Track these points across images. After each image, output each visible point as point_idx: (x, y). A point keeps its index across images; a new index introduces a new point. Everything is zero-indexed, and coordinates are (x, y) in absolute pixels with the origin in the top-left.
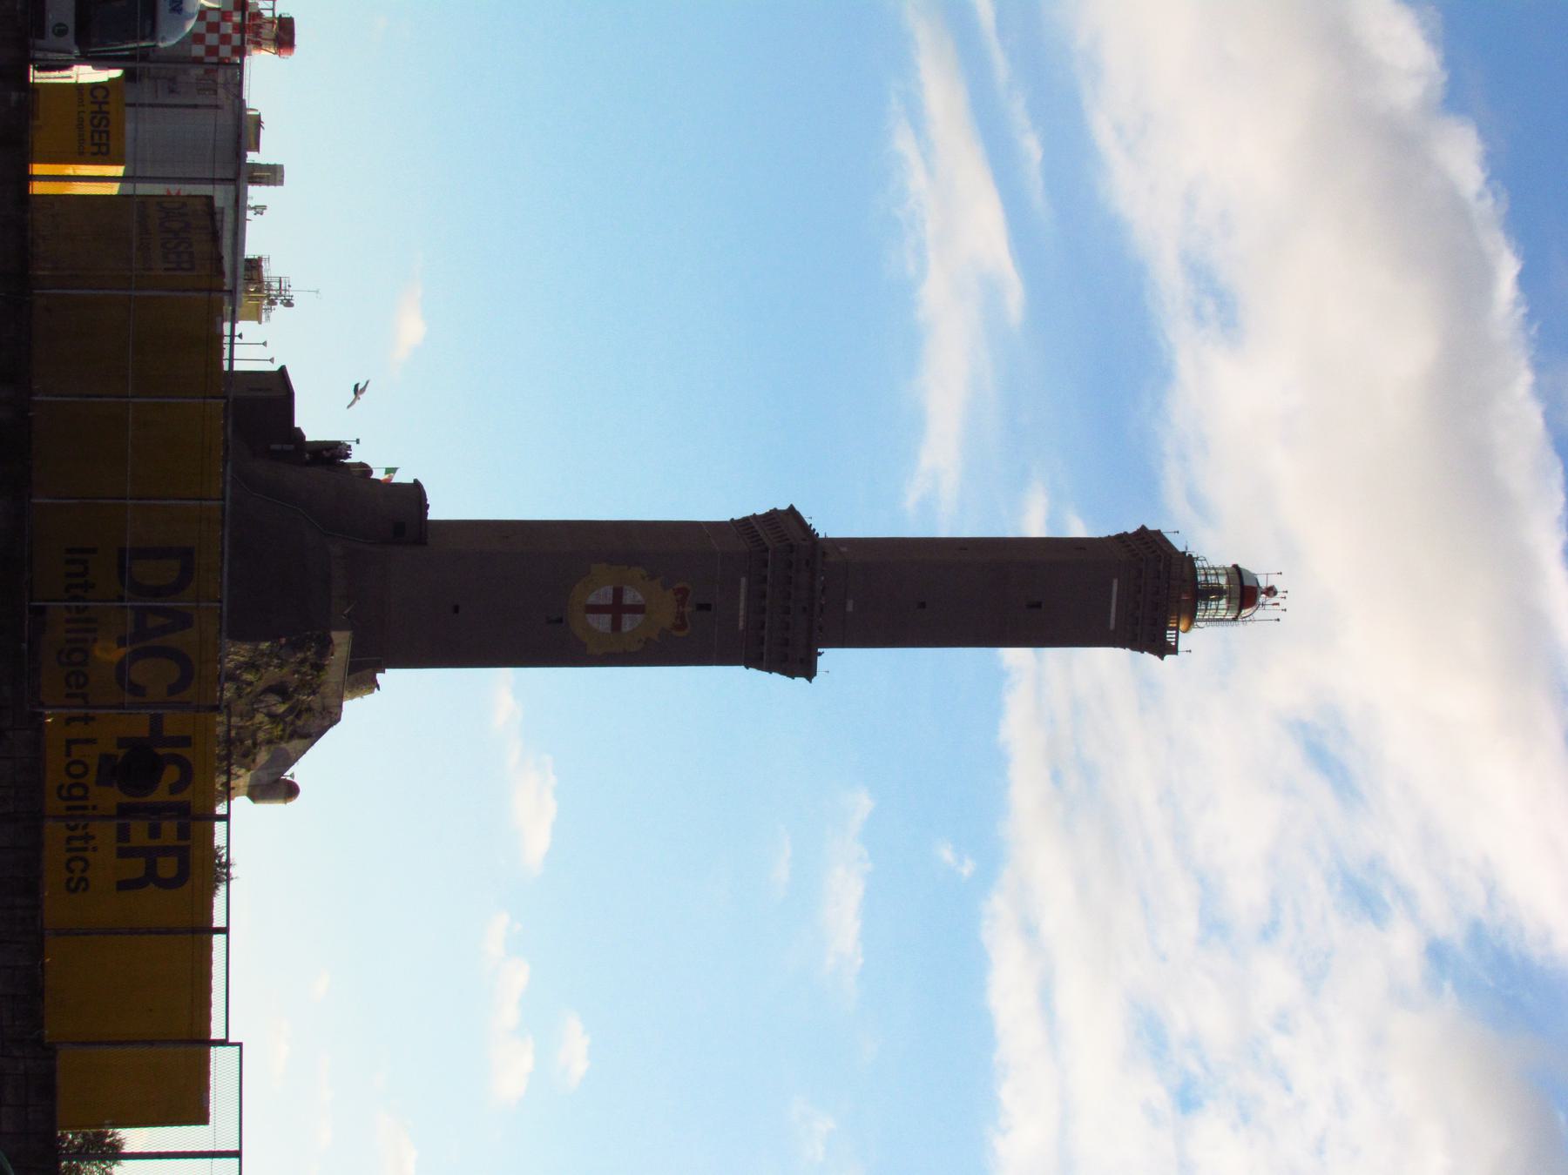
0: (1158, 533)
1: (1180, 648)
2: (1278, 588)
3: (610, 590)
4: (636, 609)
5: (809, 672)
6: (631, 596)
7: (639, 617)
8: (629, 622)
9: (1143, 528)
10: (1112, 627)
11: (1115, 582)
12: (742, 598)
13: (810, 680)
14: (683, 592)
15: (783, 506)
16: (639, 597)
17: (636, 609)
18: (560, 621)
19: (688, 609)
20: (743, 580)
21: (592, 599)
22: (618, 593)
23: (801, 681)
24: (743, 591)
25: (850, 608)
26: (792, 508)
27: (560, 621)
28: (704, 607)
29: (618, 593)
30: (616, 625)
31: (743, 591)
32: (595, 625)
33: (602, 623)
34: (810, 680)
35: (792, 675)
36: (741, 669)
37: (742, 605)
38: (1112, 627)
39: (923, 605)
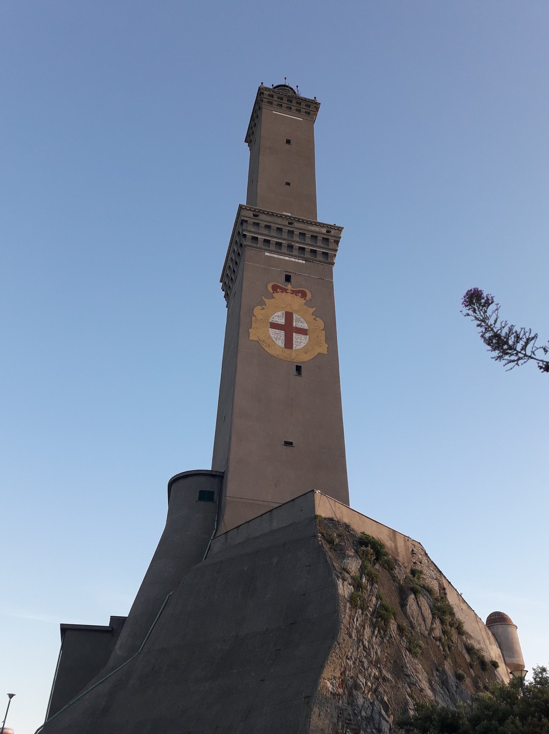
4: (289, 316)
6: (279, 318)
7: (295, 316)
13: (340, 229)
14: (275, 288)
16: (280, 313)
17: (289, 316)
18: (298, 369)
20: (267, 254)
21: (281, 343)
22: (274, 326)
23: (343, 235)
28: (288, 279)
29: (274, 326)
32: (303, 345)
34: (340, 229)
36: (335, 269)
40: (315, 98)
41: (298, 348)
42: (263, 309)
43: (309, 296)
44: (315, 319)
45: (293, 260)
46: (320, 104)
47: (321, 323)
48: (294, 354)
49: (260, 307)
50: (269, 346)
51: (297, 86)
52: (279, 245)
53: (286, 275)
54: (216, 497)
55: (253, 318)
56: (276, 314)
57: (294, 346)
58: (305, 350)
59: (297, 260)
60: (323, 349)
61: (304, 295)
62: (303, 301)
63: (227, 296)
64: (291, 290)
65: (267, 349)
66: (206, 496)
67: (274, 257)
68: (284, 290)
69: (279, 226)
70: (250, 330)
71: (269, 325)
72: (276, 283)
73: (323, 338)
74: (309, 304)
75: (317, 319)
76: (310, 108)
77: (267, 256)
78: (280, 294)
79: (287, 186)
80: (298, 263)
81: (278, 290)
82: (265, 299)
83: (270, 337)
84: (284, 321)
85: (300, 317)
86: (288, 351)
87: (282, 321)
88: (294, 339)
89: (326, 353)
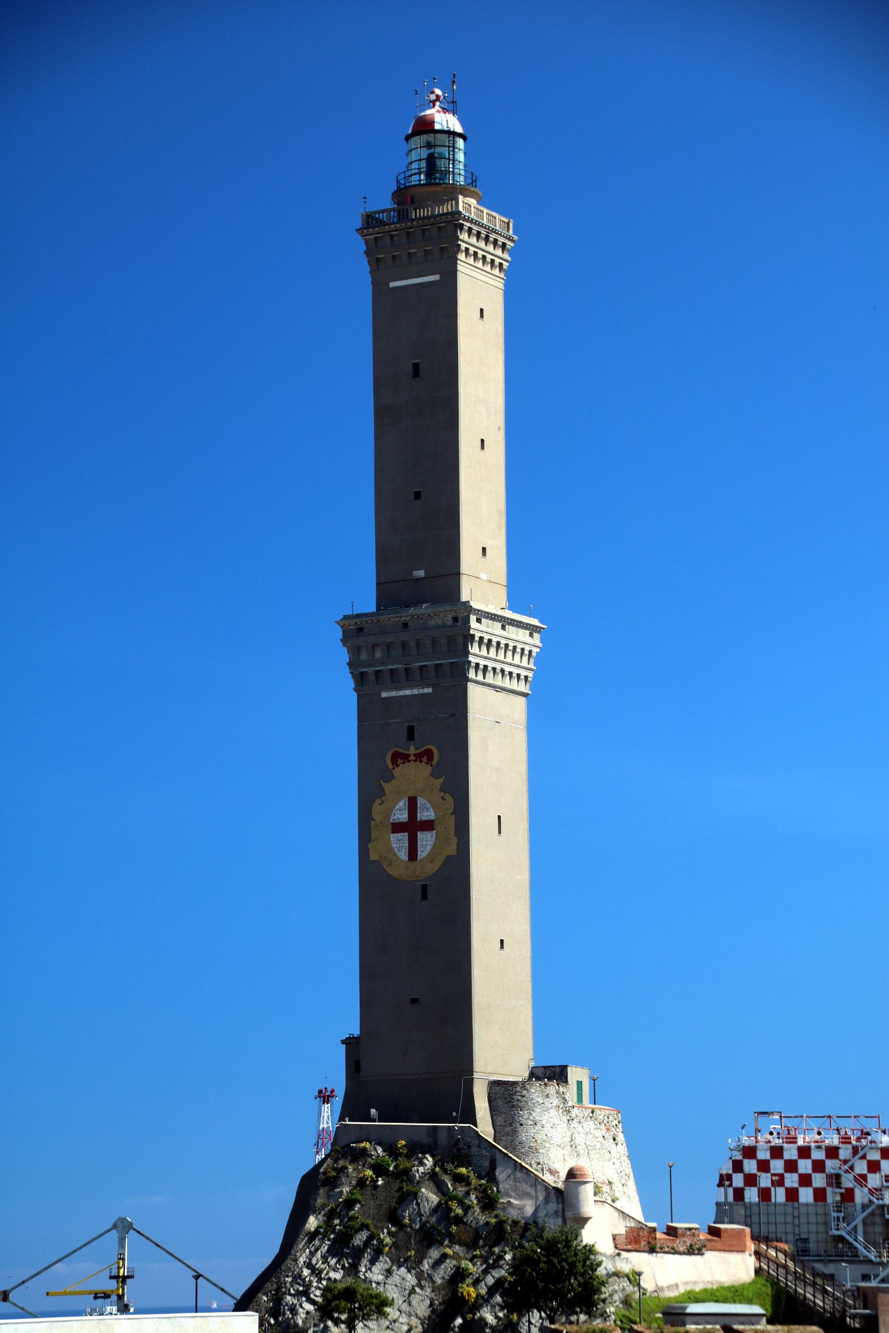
3: (394, 837)
5: (468, 609)
7: (420, 801)
8: (425, 813)
12: (401, 693)
18: (424, 888)
19: (412, 750)
21: (403, 855)
22: (397, 828)
24: (394, 694)
27: (424, 888)
28: (411, 731)
29: (397, 828)
30: (428, 826)
31: (394, 694)
32: (429, 848)
37: (408, 692)
39: (418, 495)
41: (424, 855)
42: (383, 802)
44: (443, 798)
45: (416, 691)
48: (418, 869)
49: (378, 801)
50: (390, 865)
55: (372, 822)
56: (397, 807)
57: (419, 853)
58: (432, 857)
60: (452, 850)
64: (415, 755)
65: (388, 869)
67: (392, 698)
68: (406, 758)
70: (370, 846)
75: (447, 796)
80: (423, 695)
81: (400, 761)
82: (384, 785)
83: (391, 849)
84: (406, 816)
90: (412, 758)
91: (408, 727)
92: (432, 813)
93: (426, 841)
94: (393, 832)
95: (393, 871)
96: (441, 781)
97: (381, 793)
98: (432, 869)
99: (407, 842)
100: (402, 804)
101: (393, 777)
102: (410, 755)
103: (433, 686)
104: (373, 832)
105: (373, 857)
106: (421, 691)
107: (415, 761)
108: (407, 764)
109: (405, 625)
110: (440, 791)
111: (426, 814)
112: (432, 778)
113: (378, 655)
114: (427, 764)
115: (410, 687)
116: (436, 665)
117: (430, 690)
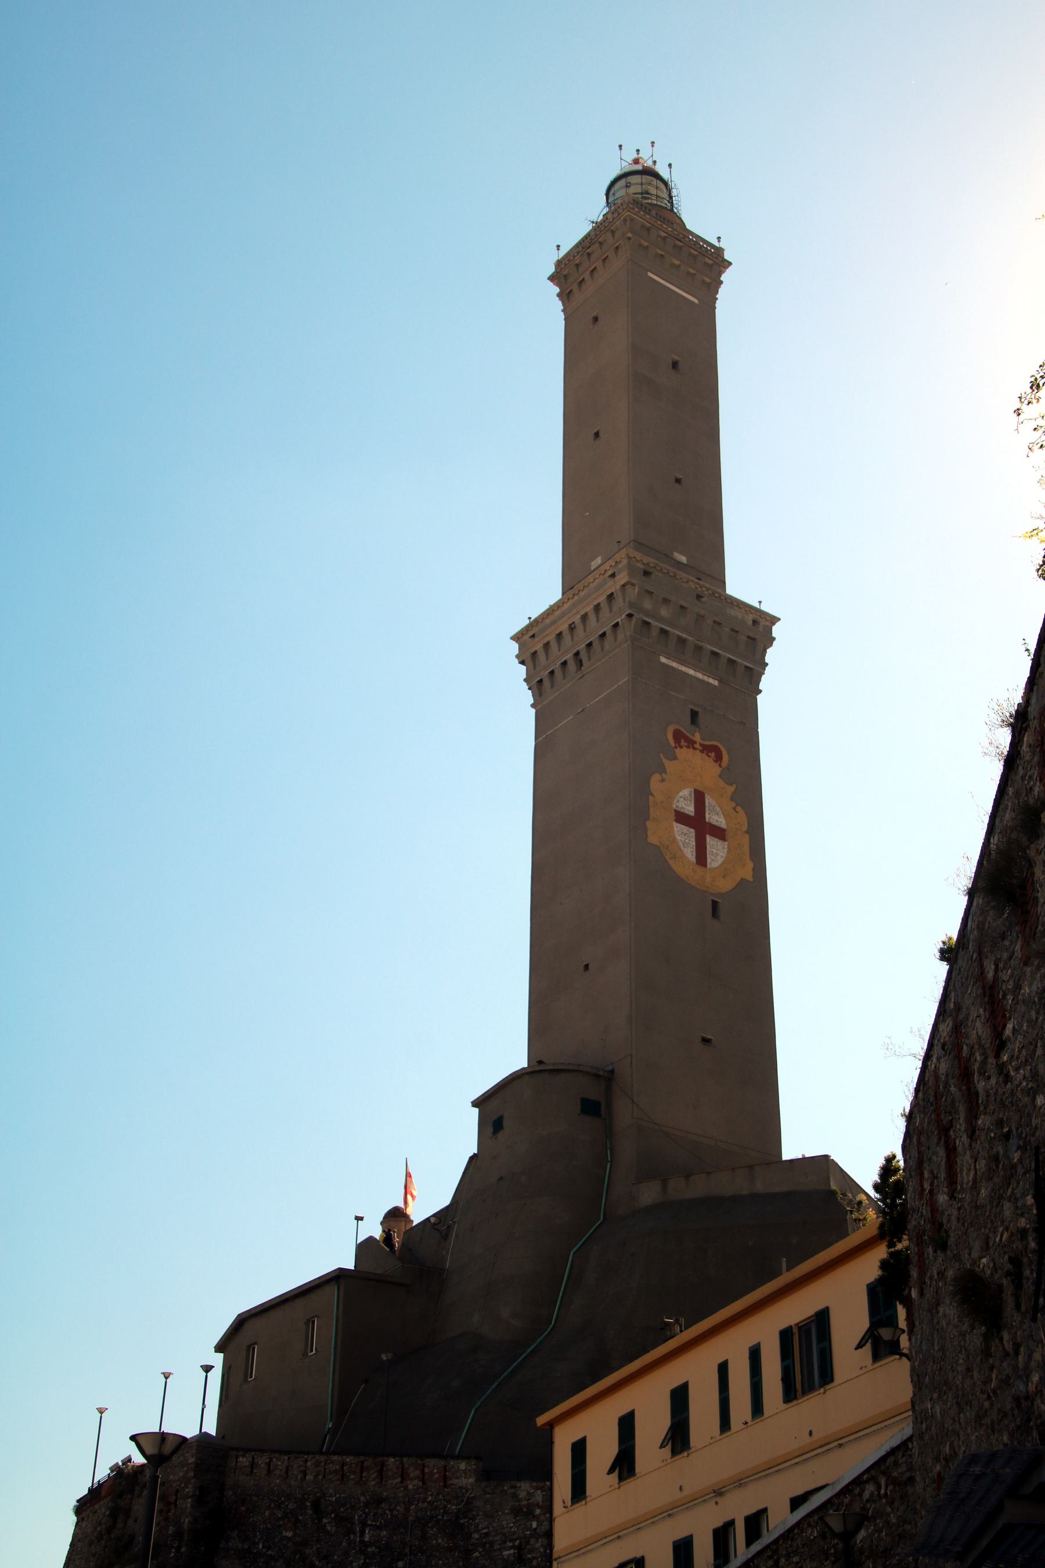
0: (559, 263)
1: (717, 244)
2: (635, 156)
7: (708, 800)
8: (715, 817)
9: (552, 278)
10: (696, 301)
11: (650, 274)
12: (683, 669)
13: (774, 620)
14: (678, 736)
15: (515, 648)
17: (699, 798)
18: (715, 904)
19: (697, 737)
20: (663, 660)
21: (690, 853)
22: (681, 818)
23: (776, 631)
24: (674, 665)
25: (683, 559)
26: (516, 638)
27: (715, 904)
29: (681, 818)
30: (720, 833)
31: (674, 665)
32: (720, 860)
33: (717, 851)
34: (774, 620)
35: (771, 640)
37: (691, 672)
38: (696, 301)
40: (719, 238)
41: (715, 865)
42: (663, 780)
43: (725, 758)
44: (734, 809)
45: (700, 676)
46: (730, 264)
47: (742, 817)
51: (670, 165)
52: (682, 641)
53: (692, 710)
54: (603, 1109)
55: (651, 798)
56: (681, 794)
57: (709, 861)
58: (725, 870)
59: (706, 678)
60: (746, 872)
61: (719, 758)
62: (718, 770)
63: (536, 685)
64: (701, 745)
65: (671, 862)
66: (590, 1108)
67: (672, 668)
68: (691, 744)
69: (684, 604)
70: (648, 824)
71: (673, 817)
72: (678, 727)
73: (746, 849)
74: (726, 776)
75: (739, 809)
76: (706, 264)
77: (664, 664)
78: (684, 749)
79: (677, 485)
80: (709, 684)
81: (683, 743)
82: (665, 761)
83: (674, 840)
85: (713, 803)
86: (698, 868)
87: (690, 809)
88: (708, 847)
89: (751, 879)
90: (697, 746)
91: (692, 710)
92: (723, 821)
93: (717, 851)
94: (677, 821)
95: (677, 867)
96: (732, 788)
97: (662, 770)
98: (725, 885)
99: (693, 839)
100: (686, 792)
101: (675, 758)
102: (695, 742)
103: (720, 681)
104: (651, 809)
105: (653, 839)
106: (706, 678)
107: (702, 752)
108: (691, 750)
109: (699, 597)
110: (732, 799)
111: (715, 817)
112: (721, 783)
113: (664, 612)
114: (716, 761)
115: (695, 668)
116: (730, 660)
117: (716, 683)
